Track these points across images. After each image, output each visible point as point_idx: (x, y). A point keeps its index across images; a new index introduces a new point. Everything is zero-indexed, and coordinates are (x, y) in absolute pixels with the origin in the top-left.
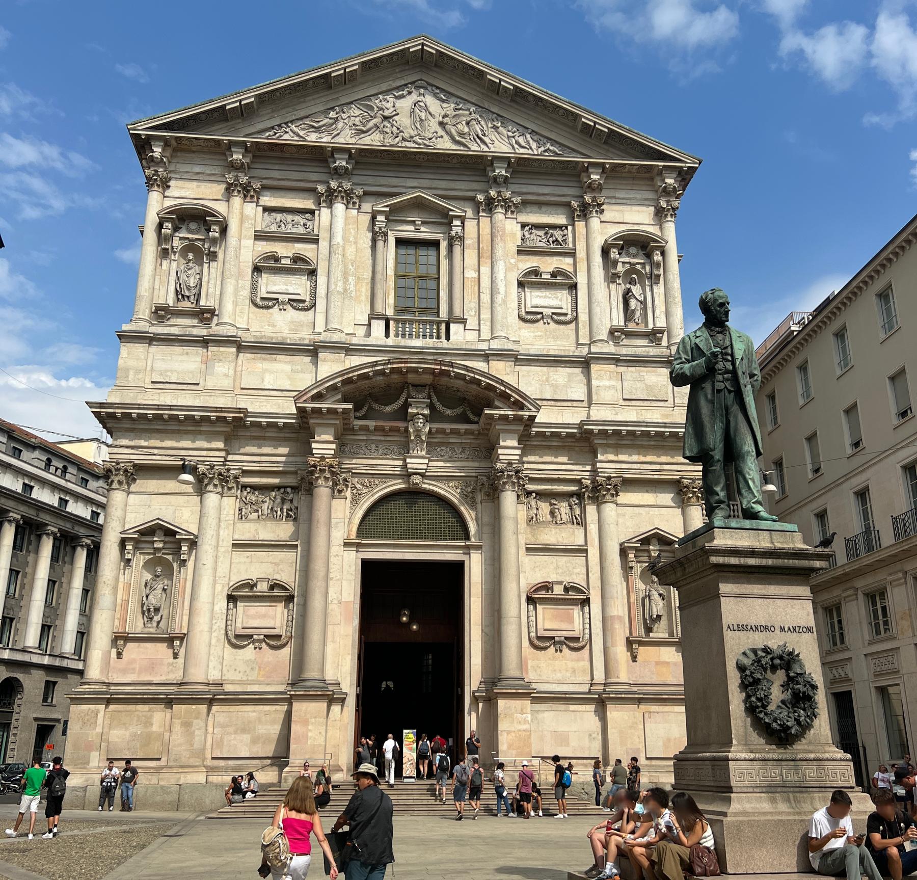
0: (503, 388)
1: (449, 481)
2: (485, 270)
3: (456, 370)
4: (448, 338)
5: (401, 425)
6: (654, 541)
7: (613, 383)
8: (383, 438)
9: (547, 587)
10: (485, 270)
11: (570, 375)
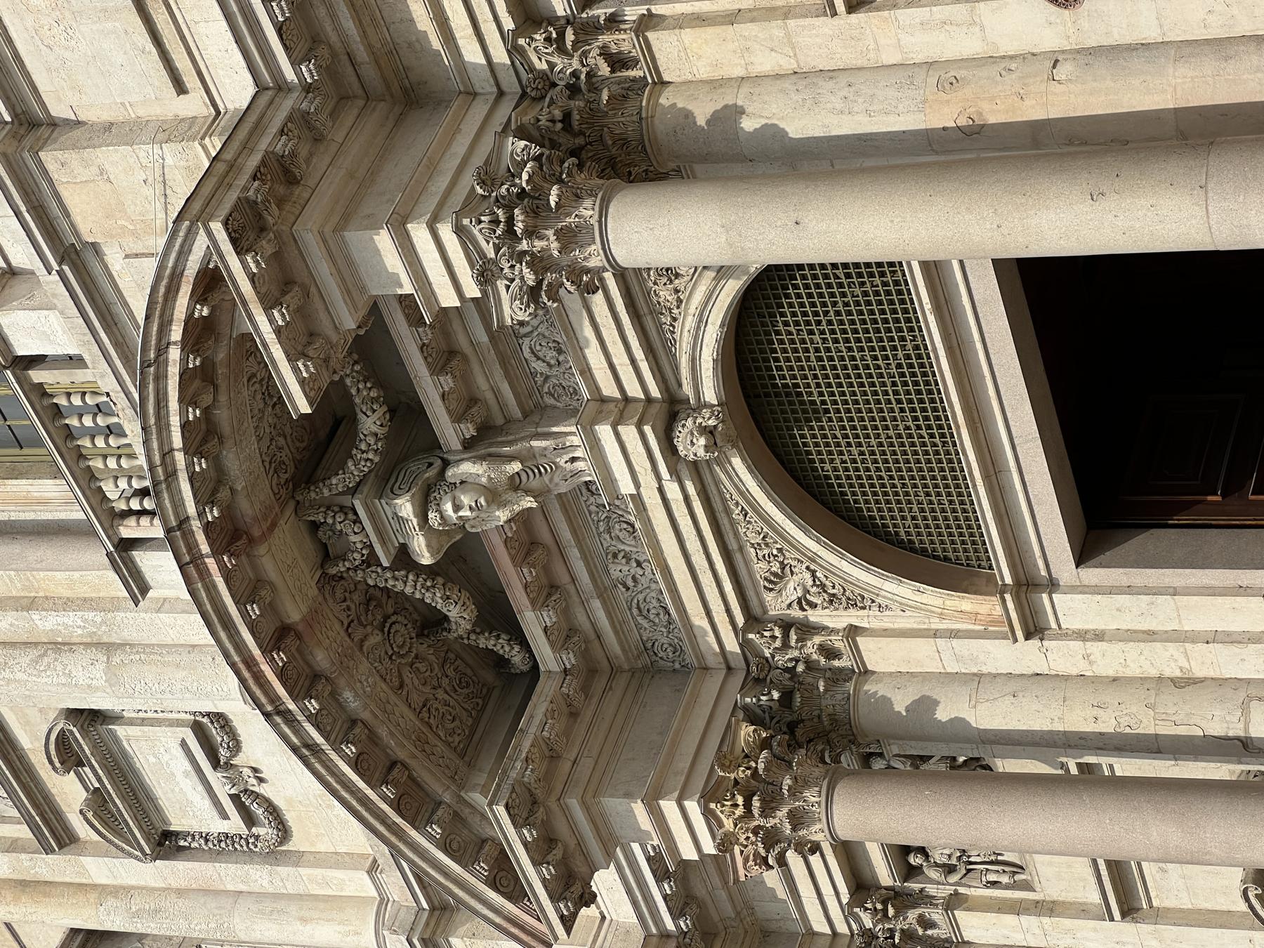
0: (174, 354)
1: (656, 312)
3: (191, 509)
8: (574, 554)
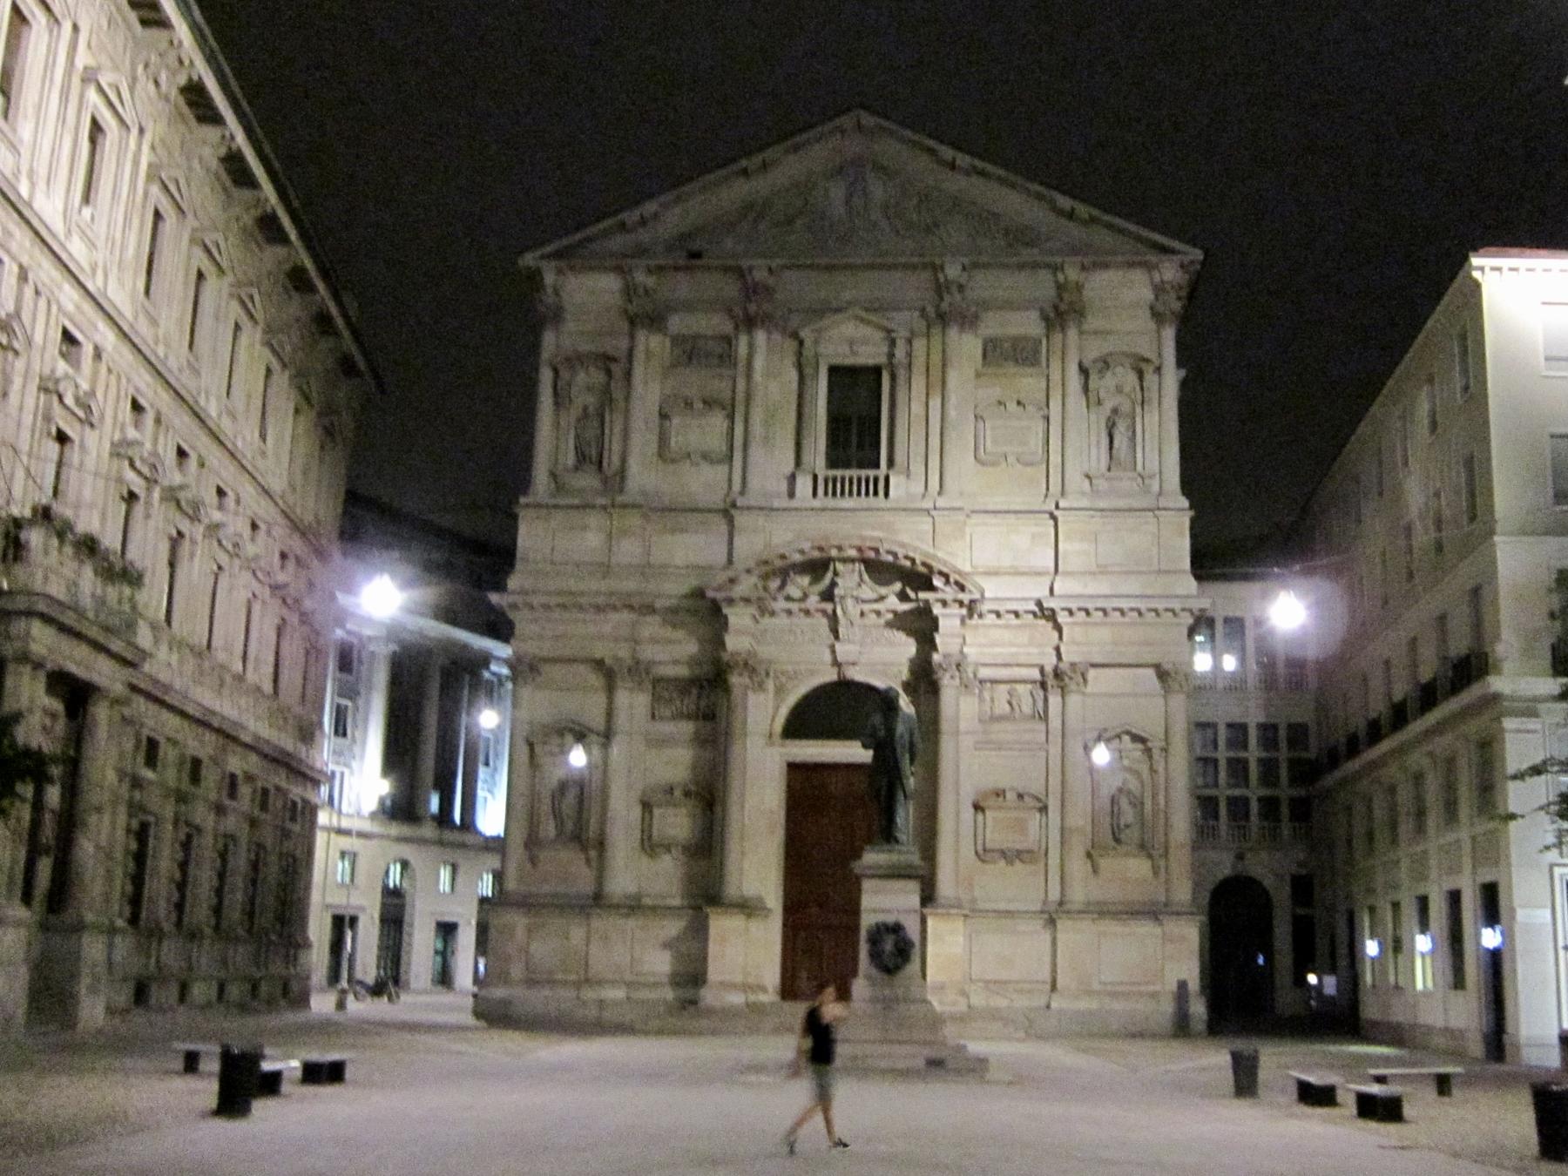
2: (935, 403)
4: (887, 494)
5: (829, 607)
6: (1126, 738)
7: (1085, 546)
9: (1000, 793)
10: (935, 403)
11: (1033, 536)
